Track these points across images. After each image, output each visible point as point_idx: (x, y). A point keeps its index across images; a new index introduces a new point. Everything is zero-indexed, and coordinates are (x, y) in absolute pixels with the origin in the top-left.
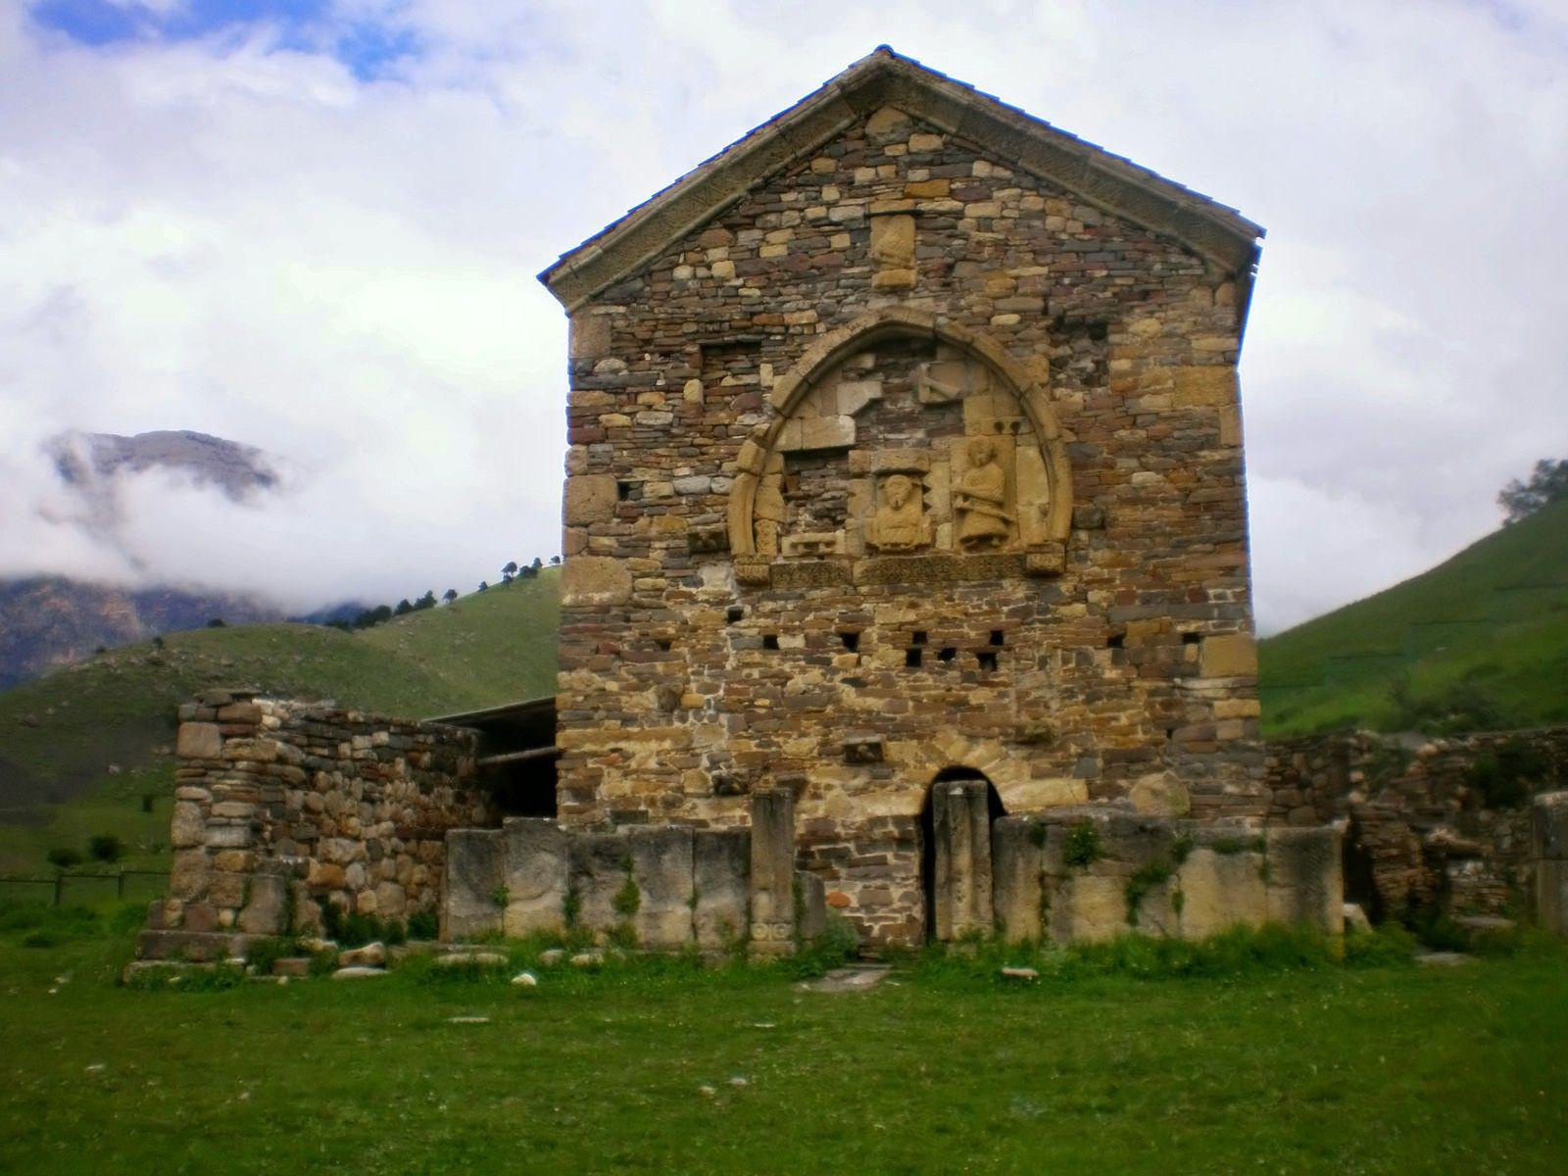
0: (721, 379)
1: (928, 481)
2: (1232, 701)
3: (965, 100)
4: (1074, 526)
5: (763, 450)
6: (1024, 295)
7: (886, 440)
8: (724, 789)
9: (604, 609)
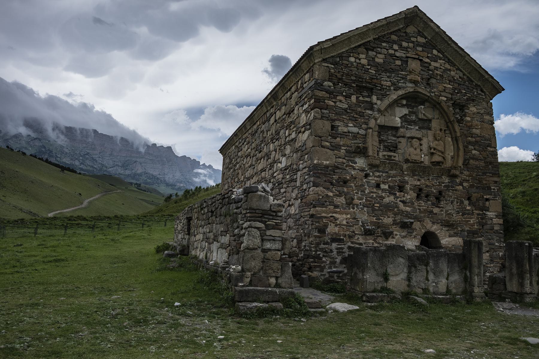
0: (359, 97)
2: (497, 219)
3: (437, 30)
6: (447, 92)
7: (407, 127)
8: (368, 233)
9: (327, 167)
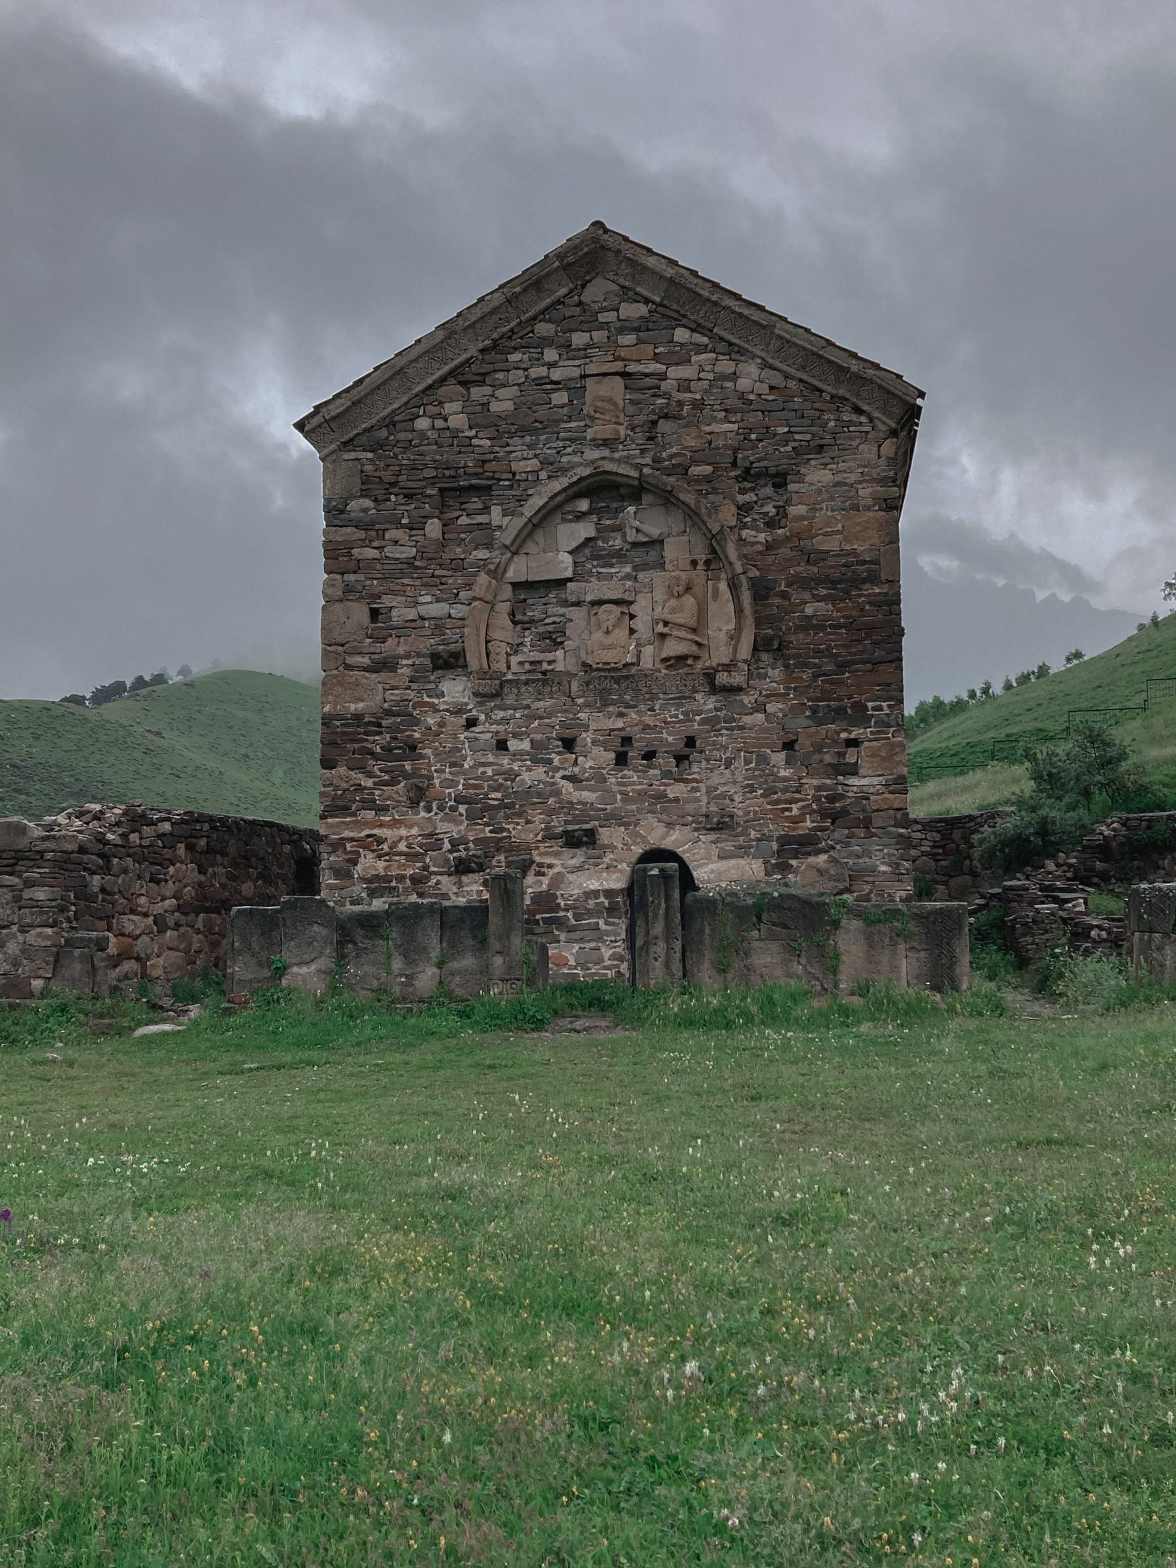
0: (457, 518)
1: (634, 609)
3: (670, 272)
4: (756, 649)
5: (494, 581)
8: (462, 868)
9: (358, 717)
